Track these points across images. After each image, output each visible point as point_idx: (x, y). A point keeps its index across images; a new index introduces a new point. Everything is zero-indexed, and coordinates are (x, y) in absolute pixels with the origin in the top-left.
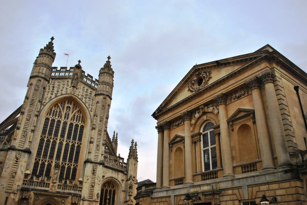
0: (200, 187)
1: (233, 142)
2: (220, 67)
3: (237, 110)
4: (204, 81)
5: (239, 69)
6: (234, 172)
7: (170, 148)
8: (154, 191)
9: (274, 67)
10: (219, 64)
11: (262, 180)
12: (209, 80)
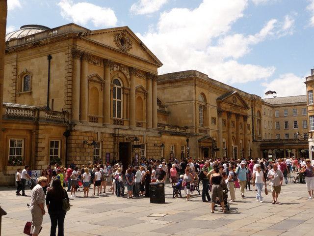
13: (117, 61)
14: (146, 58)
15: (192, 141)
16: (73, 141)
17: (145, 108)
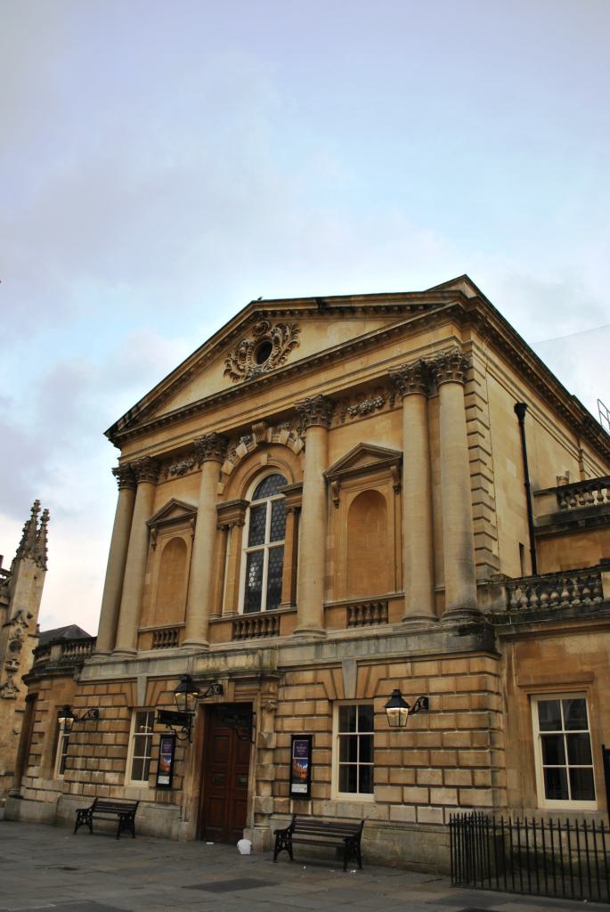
0: (226, 657)
1: (333, 537)
2: (327, 316)
3: (356, 449)
4: (274, 352)
5: (378, 332)
6: (326, 621)
7: (151, 538)
8: (87, 662)
9: (472, 343)
10: (325, 309)
11: (399, 648)
12: (290, 351)
13: (234, 424)
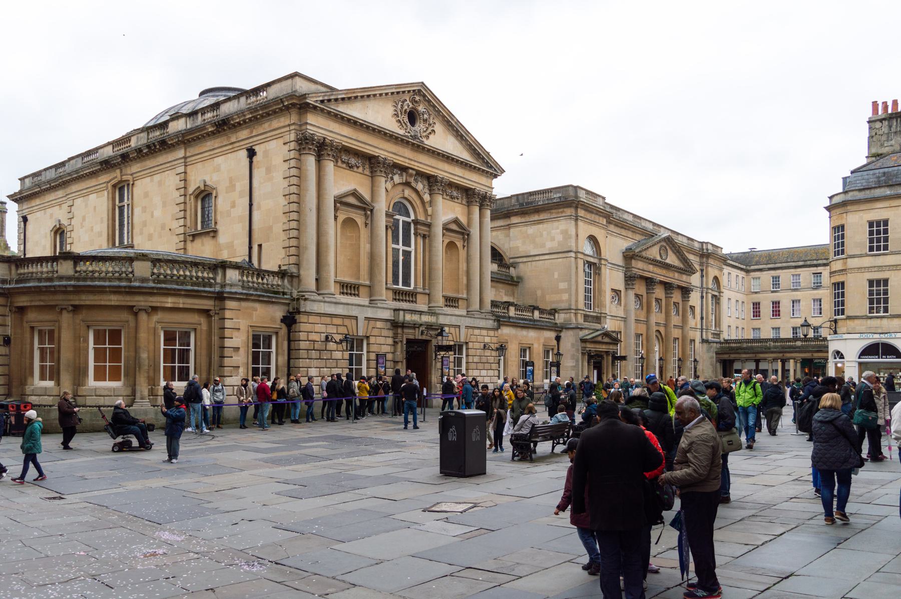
14: (464, 155)
15: (569, 340)
16: (303, 336)
17: (463, 266)
